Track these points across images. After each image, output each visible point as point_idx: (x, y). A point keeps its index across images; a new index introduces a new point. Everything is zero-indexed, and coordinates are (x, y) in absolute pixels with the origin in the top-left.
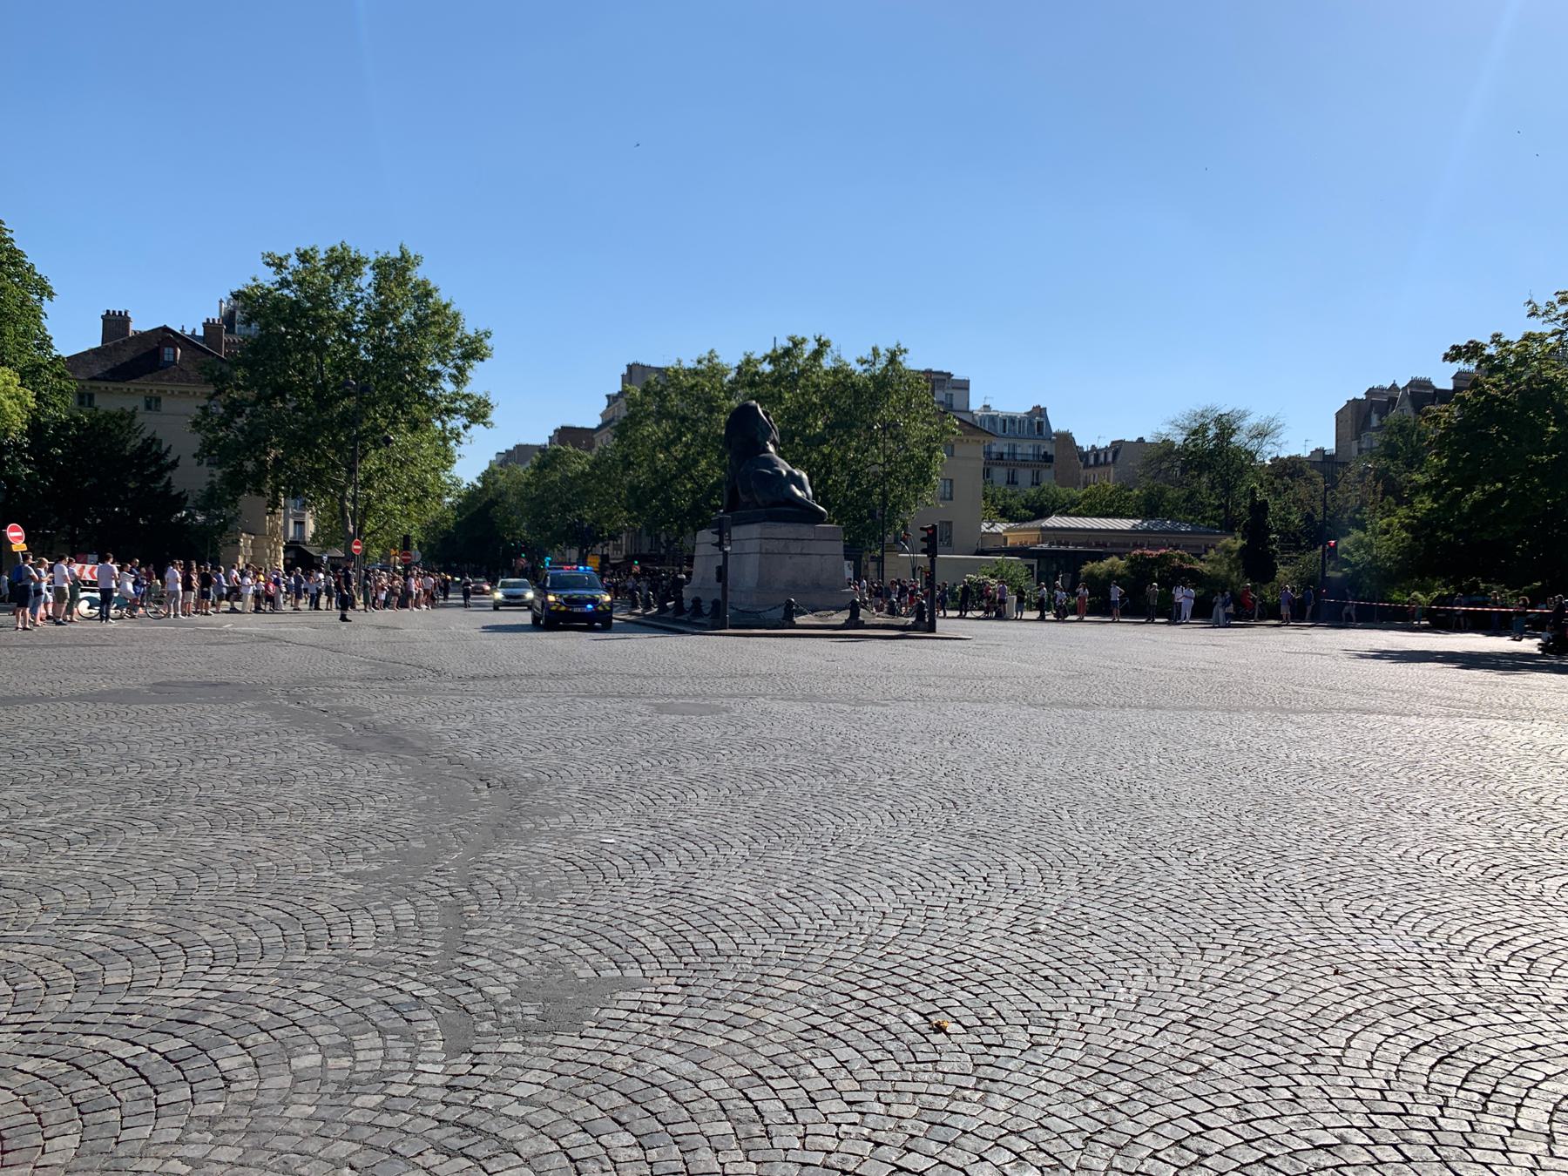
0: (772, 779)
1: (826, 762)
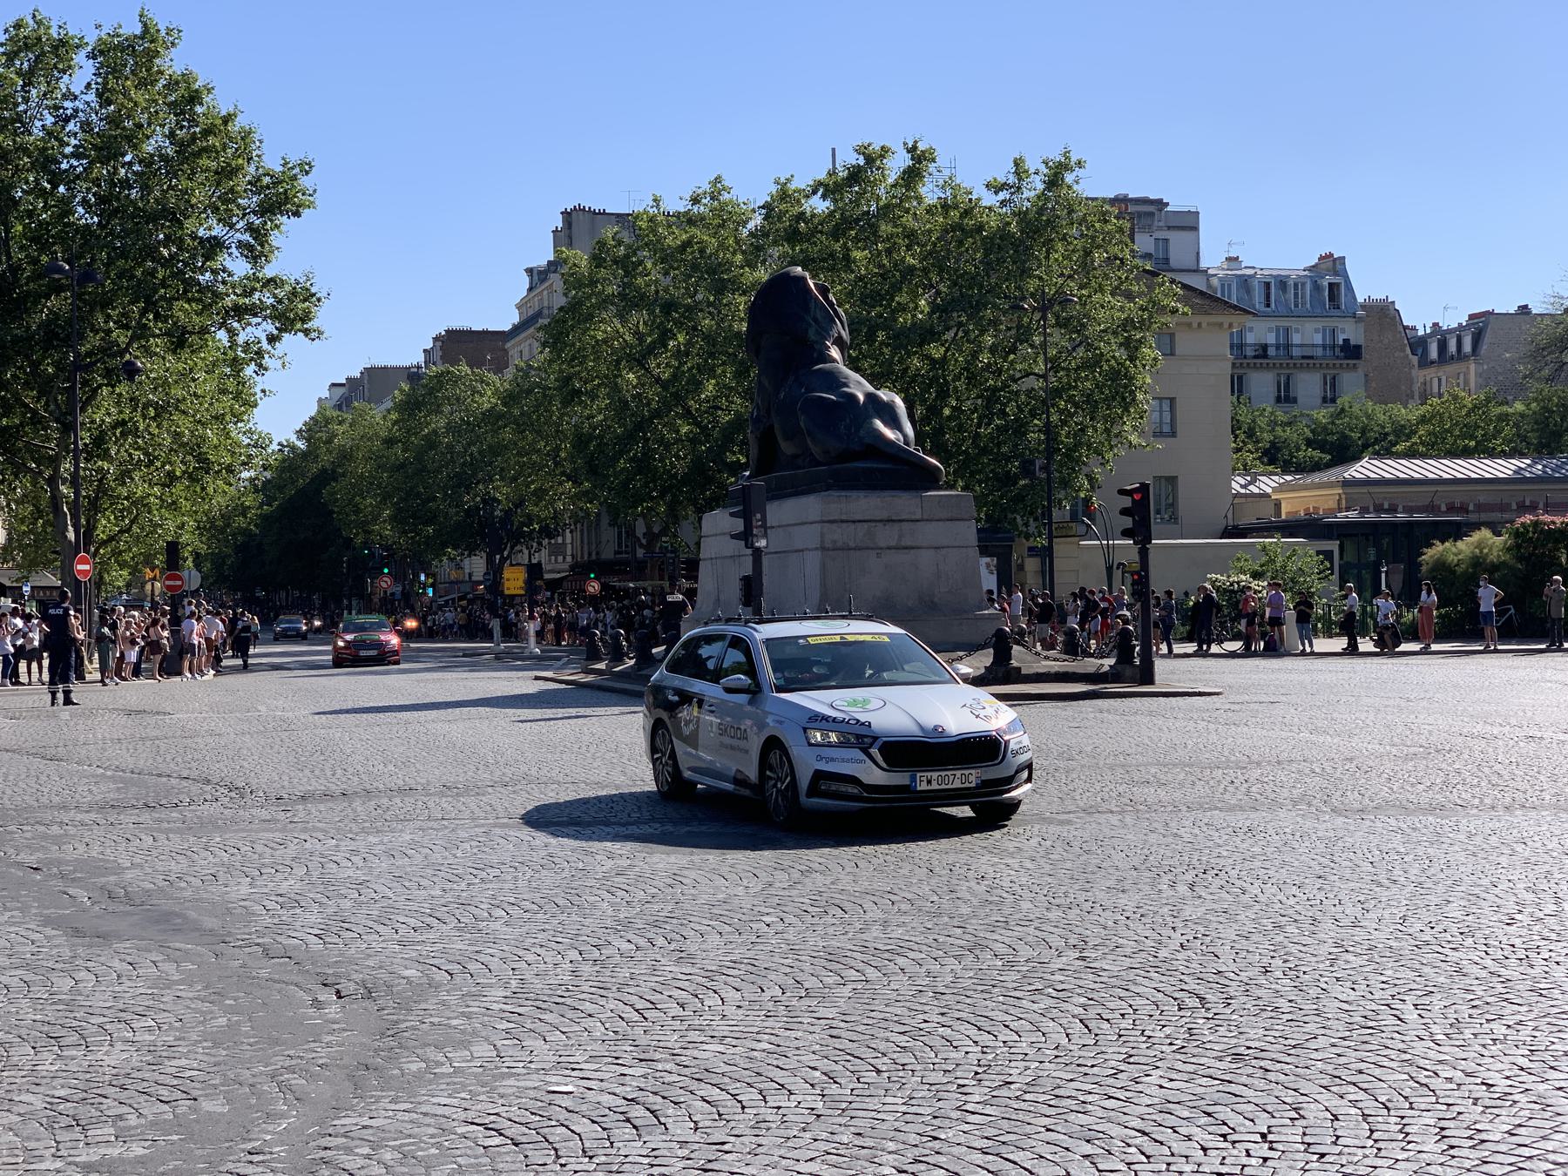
0: (861, 966)
1: (959, 931)
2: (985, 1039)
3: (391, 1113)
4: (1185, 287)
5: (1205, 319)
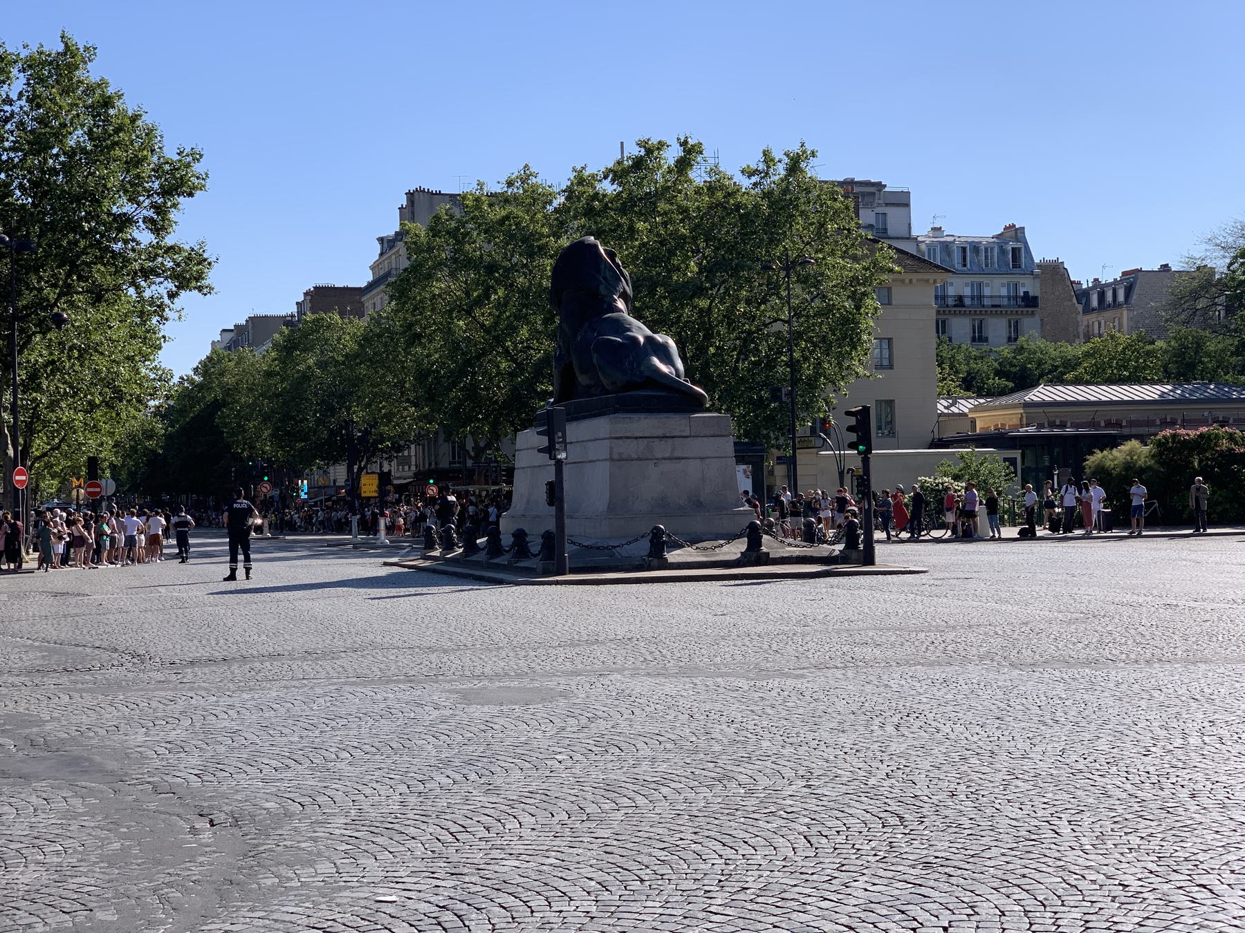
0: (632, 794)
1: (712, 764)
2: (728, 852)
3: (248, 920)
4: (899, 251)
5: (915, 277)
